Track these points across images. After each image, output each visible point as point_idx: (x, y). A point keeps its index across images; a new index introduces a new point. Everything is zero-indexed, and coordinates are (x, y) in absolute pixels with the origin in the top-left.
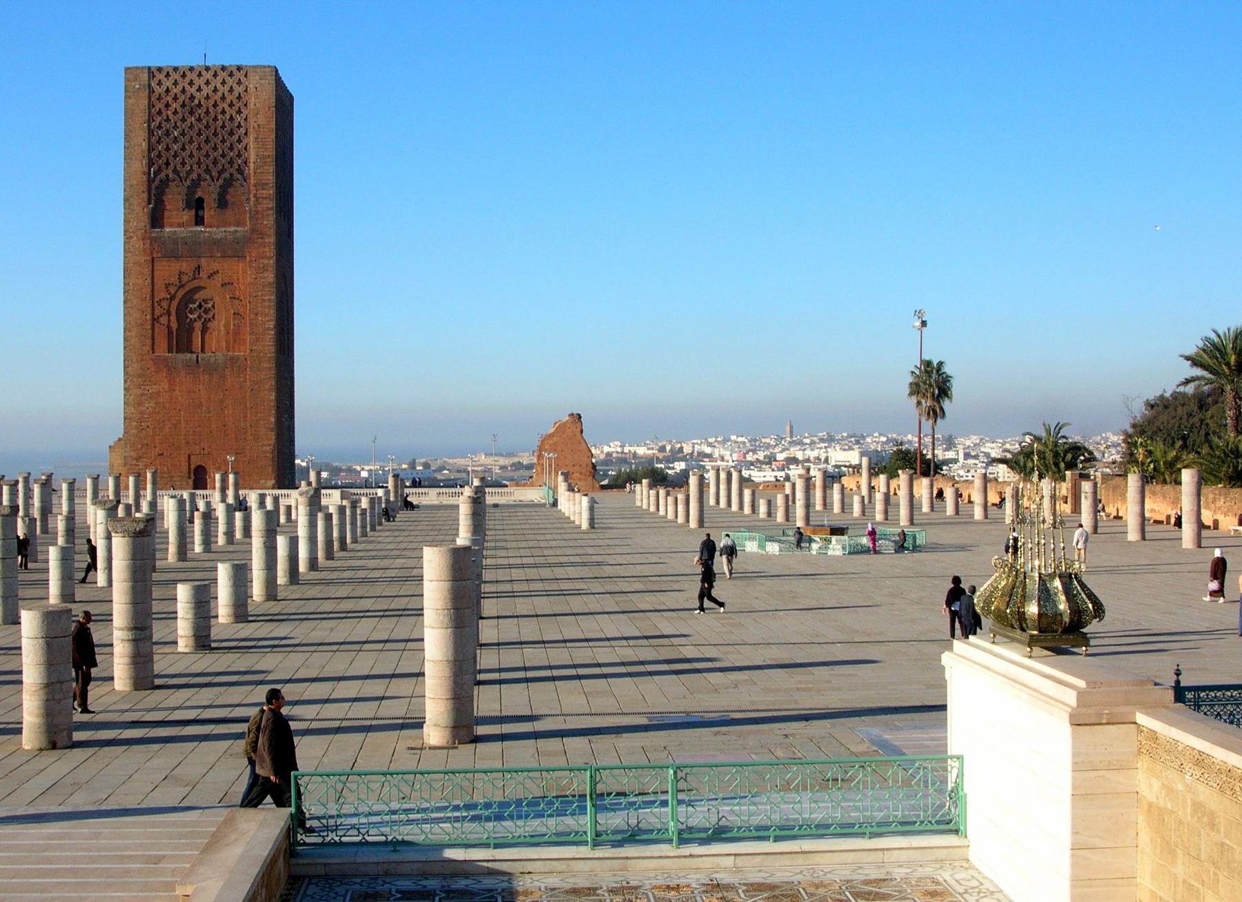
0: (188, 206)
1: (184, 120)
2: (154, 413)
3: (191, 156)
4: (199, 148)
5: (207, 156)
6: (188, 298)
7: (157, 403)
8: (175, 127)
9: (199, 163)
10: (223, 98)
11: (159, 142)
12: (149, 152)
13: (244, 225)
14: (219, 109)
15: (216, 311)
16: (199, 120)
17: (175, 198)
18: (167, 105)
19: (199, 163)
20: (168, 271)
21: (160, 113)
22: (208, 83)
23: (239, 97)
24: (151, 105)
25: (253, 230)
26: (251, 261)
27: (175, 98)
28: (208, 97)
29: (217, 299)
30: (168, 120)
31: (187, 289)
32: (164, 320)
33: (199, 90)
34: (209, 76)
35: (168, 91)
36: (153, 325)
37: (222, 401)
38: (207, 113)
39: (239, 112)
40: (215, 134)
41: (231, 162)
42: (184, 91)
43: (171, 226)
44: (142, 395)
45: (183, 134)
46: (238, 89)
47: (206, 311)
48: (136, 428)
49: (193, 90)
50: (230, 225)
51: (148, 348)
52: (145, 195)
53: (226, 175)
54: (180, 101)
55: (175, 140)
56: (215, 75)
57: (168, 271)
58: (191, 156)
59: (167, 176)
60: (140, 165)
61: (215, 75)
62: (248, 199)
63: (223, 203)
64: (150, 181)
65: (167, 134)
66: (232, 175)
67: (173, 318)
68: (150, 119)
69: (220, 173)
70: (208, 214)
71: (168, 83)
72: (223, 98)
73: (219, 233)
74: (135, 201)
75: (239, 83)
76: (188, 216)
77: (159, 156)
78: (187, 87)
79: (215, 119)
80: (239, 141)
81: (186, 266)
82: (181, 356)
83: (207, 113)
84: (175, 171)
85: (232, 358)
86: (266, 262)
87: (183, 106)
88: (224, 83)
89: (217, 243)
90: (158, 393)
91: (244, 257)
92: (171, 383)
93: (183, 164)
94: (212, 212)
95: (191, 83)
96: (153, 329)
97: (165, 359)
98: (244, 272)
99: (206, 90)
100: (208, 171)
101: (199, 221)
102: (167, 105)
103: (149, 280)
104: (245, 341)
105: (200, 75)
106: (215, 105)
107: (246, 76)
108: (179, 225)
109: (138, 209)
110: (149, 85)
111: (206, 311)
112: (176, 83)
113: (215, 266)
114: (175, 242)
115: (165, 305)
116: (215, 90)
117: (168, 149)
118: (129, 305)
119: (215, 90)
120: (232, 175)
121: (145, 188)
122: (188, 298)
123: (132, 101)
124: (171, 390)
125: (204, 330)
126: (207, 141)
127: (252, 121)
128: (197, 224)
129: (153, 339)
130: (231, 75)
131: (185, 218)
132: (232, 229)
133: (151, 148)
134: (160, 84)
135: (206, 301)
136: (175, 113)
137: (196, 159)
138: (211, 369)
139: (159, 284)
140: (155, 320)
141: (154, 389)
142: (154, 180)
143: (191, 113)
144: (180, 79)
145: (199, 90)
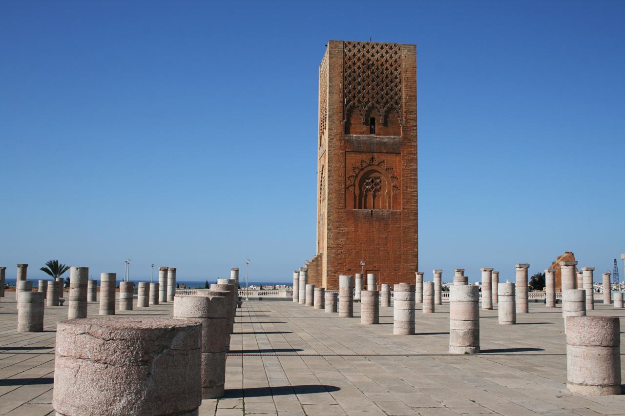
0: (366, 123)
1: (364, 72)
2: (344, 245)
3: (368, 93)
4: (373, 89)
5: (378, 93)
6: (366, 176)
7: (347, 239)
8: (359, 76)
9: (373, 98)
10: (387, 61)
11: (349, 84)
12: (344, 90)
13: (399, 135)
14: (384, 67)
15: (382, 184)
16: (373, 73)
17: (358, 120)
18: (354, 63)
19: (373, 98)
20: (354, 159)
21: (350, 67)
22: (377, 52)
23: (396, 61)
24: (345, 63)
25: (405, 138)
26: (403, 156)
27: (359, 60)
28: (378, 60)
29: (383, 178)
30: (354, 72)
31: (366, 170)
32: (351, 189)
33: (373, 56)
34: (378, 48)
35: (354, 55)
36: (345, 191)
37: (386, 238)
38: (378, 69)
39: (396, 70)
40: (382, 81)
41: (391, 98)
42: (364, 56)
43: (356, 133)
44: (339, 233)
45: (363, 80)
46: (395, 57)
47: (377, 184)
48: (335, 253)
49: (369, 55)
50: (390, 134)
51: (342, 205)
52: (341, 114)
53: (388, 105)
54: (362, 61)
55: (359, 84)
56: (382, 48)
57: (354, 159)
58: (368, 93)
59: (354, 104)
60: (337, 97)
61: (382, 48)
62: (402, 120)
63: (385, 124)
64: (344, 106)
65: (354, 80)
66: (392, 105)
67: (357, 188)
68: (344, 71)
69: (386, 103)
70: (377, 128)
71: (355, 51)
72: (387, 61)
73: (385, 139)
74: (335, 118)
75: (396, 53)
76: (365, 128)
77: (350, 92)
78: (366, 54)
79: (382, 73)
80: (396, 86)
81: (366, 157)
82: (363, 210)
83: (378, 69)
84: (359, 101)
85: (392, 213)
86: (412, 156)
87: (364, 64)
88: (387, 52)
89: (385, 143)
90: (348, 233)
91: (400, 154)
92: (356, 226)
93: (364, 97)
94: (380, 126)
95: (368, 52)
96: (345, 193)
97: (353, 212)
98: (400, 162)
99: (377, 56)
100: (378, 102)
101: (372, 131)
102: (354, 63)
103: (343, 165)
104: (400, 202)
105: (373, 47)
106: (382, 65)
107: (399, 49)
108: (361, 133)
109: (337, 122)
110: (344, 51)
111: (377, 184)
112: (359, 51)
113: (383, 157)
114: (359, 142)
115: (352, 179)
116: (382, 57)
117: (354, 88)
118: (331, 178)
119: (382, 57)
120: (392, 105)
121: (341, 110)
122: (366, 176)
123: (334, 60)
124: (356, 231)
125: (374, 196)
126: (377, 85)
127: (403, 75)
128: (371, 133)
129: (345, 198)
130: (391, 48)
131: (364, 129)
132: (392, 137)
133: (344, 87)
134: (350, 51)
135: (376, 178)
136: (359, 68)
137: (371, 95)
138: (380, 219)
139: (349, 167)
140: (346, 188)
141: (346, 230)
142: (346, 107)
143: (368, 68)
144: (361, 49)
145: (373, 56)
